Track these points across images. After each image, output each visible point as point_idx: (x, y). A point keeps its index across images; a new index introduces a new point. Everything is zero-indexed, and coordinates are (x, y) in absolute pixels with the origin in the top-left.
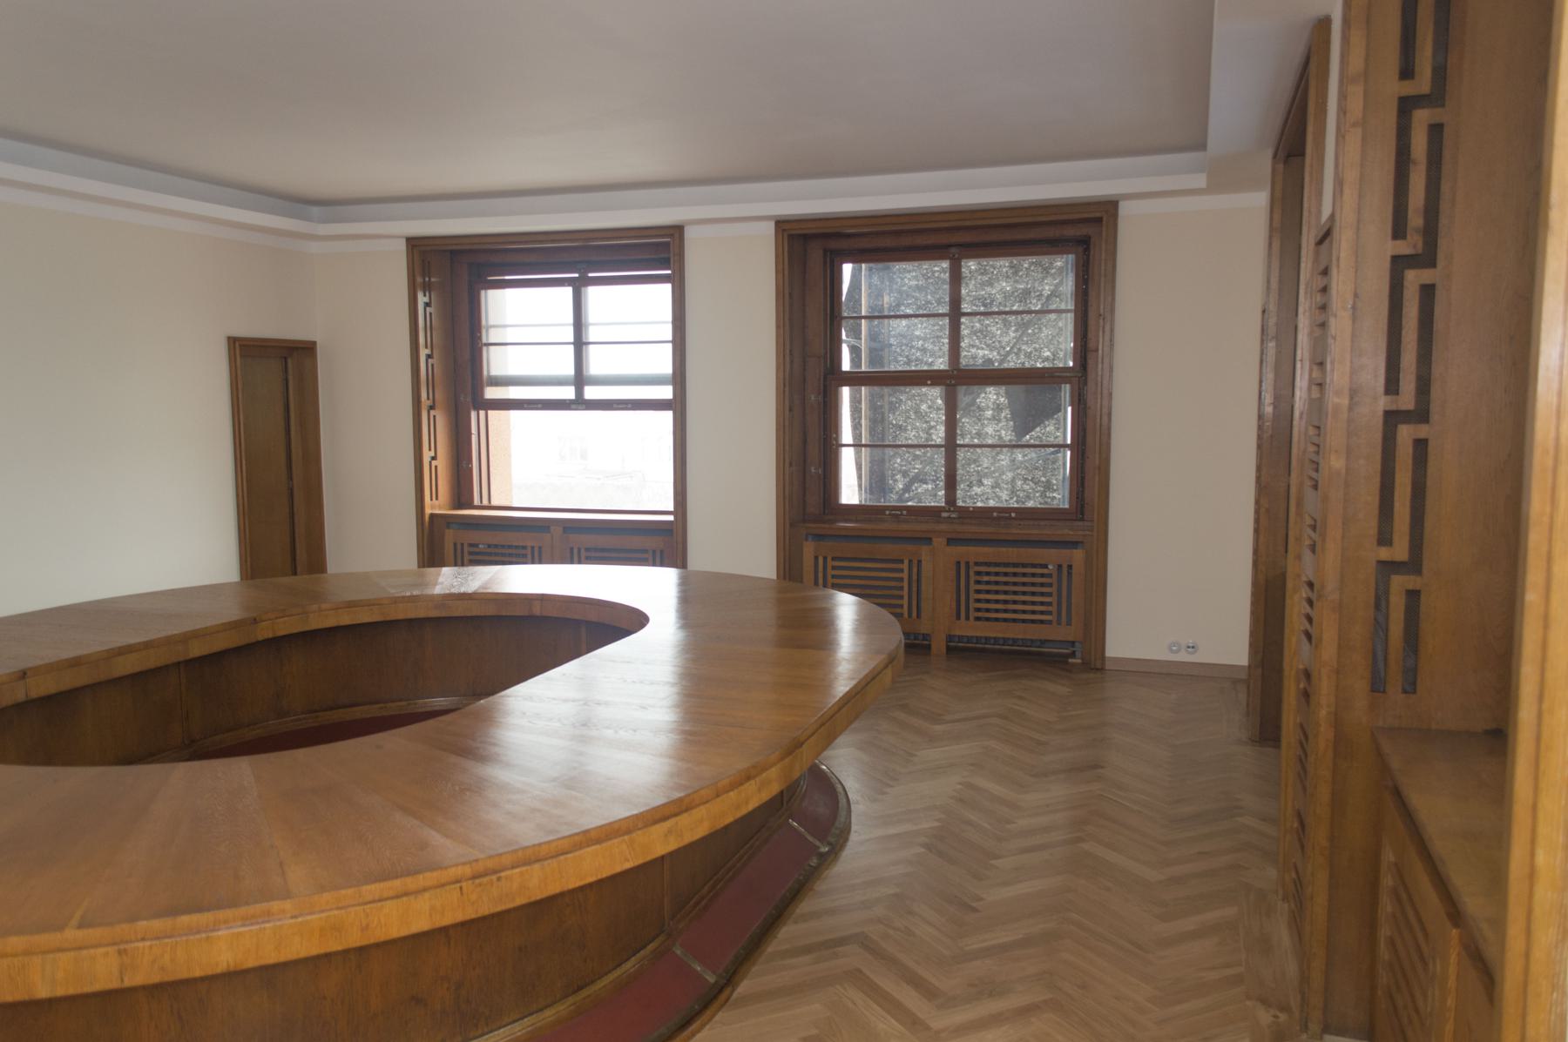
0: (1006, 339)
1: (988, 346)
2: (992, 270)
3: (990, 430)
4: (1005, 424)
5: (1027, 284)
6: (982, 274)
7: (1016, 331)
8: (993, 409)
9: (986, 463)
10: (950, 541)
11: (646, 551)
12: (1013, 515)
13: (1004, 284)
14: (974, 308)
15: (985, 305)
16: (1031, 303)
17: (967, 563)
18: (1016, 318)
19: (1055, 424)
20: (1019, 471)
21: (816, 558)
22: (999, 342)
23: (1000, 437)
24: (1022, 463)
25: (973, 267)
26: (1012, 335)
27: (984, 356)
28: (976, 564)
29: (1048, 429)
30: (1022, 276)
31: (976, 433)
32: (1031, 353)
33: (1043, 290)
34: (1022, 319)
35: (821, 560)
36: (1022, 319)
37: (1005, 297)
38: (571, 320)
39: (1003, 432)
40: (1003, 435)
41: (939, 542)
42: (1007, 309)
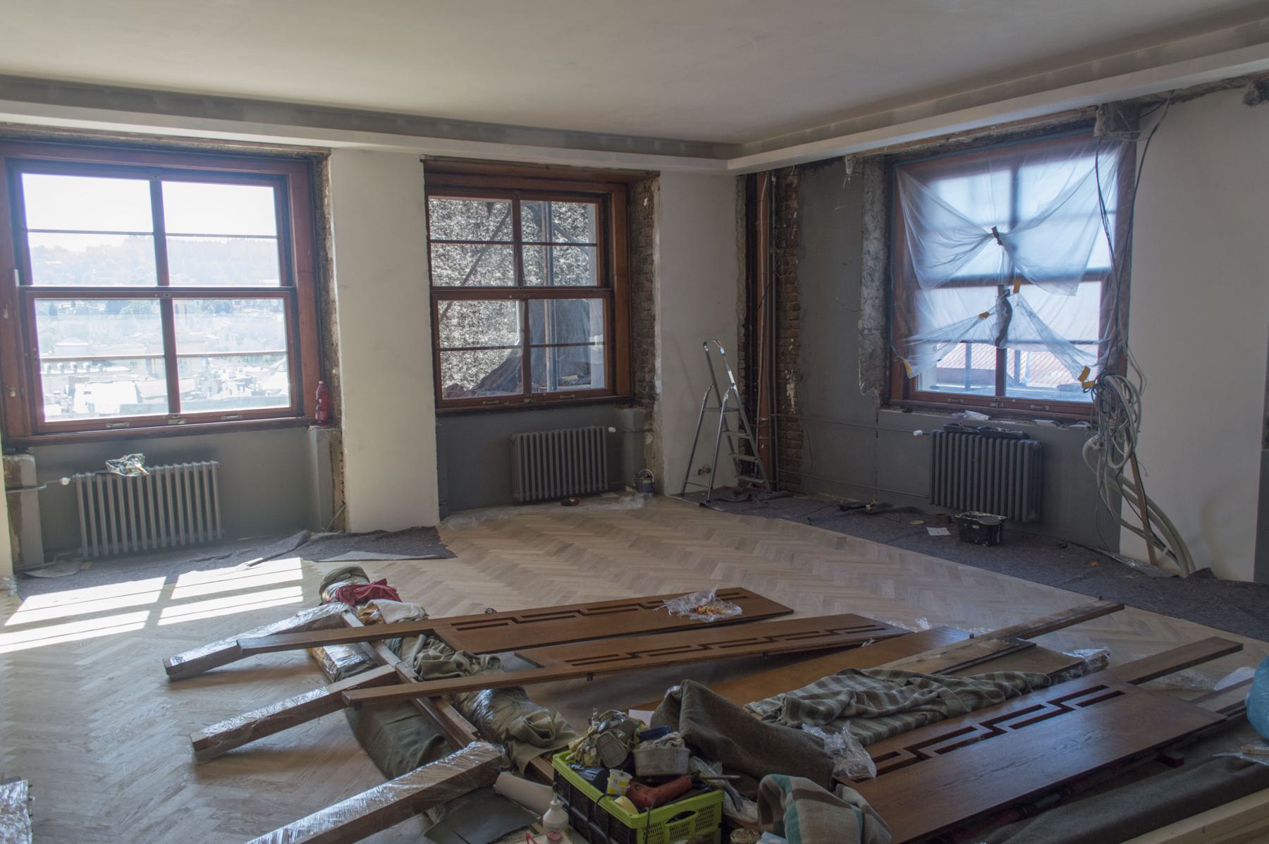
0: (465, 262)
1: (451, 267)
2: (450, 206)
3: (456, 334)
4: (468, 329)
5: (477, 218)
6: (442, 208)
7: (472, 256)
8: (458, 317)
9: (455, 361)
12: (573, 396)
13: (460, 218)
14: (437, 236)
15: (446, 235)
16: (481, 235)
18: (471, 246)
19: (507, 328)
20: (481, 366)
22: (460, 264)
23: (465, 340)
24: (482, 360)
25: (435, 202)
26: (469, 259)
27: (447, 276)
29: (502, 332)
30: (472, 213)
31: (445, 338)
32: (485, 273)
33: (489, 225)
34: (476, 248)
36: (476, 248)
37: (461, 229)
39: (467, 336)
40: (467, 338)
42: (464, 239)
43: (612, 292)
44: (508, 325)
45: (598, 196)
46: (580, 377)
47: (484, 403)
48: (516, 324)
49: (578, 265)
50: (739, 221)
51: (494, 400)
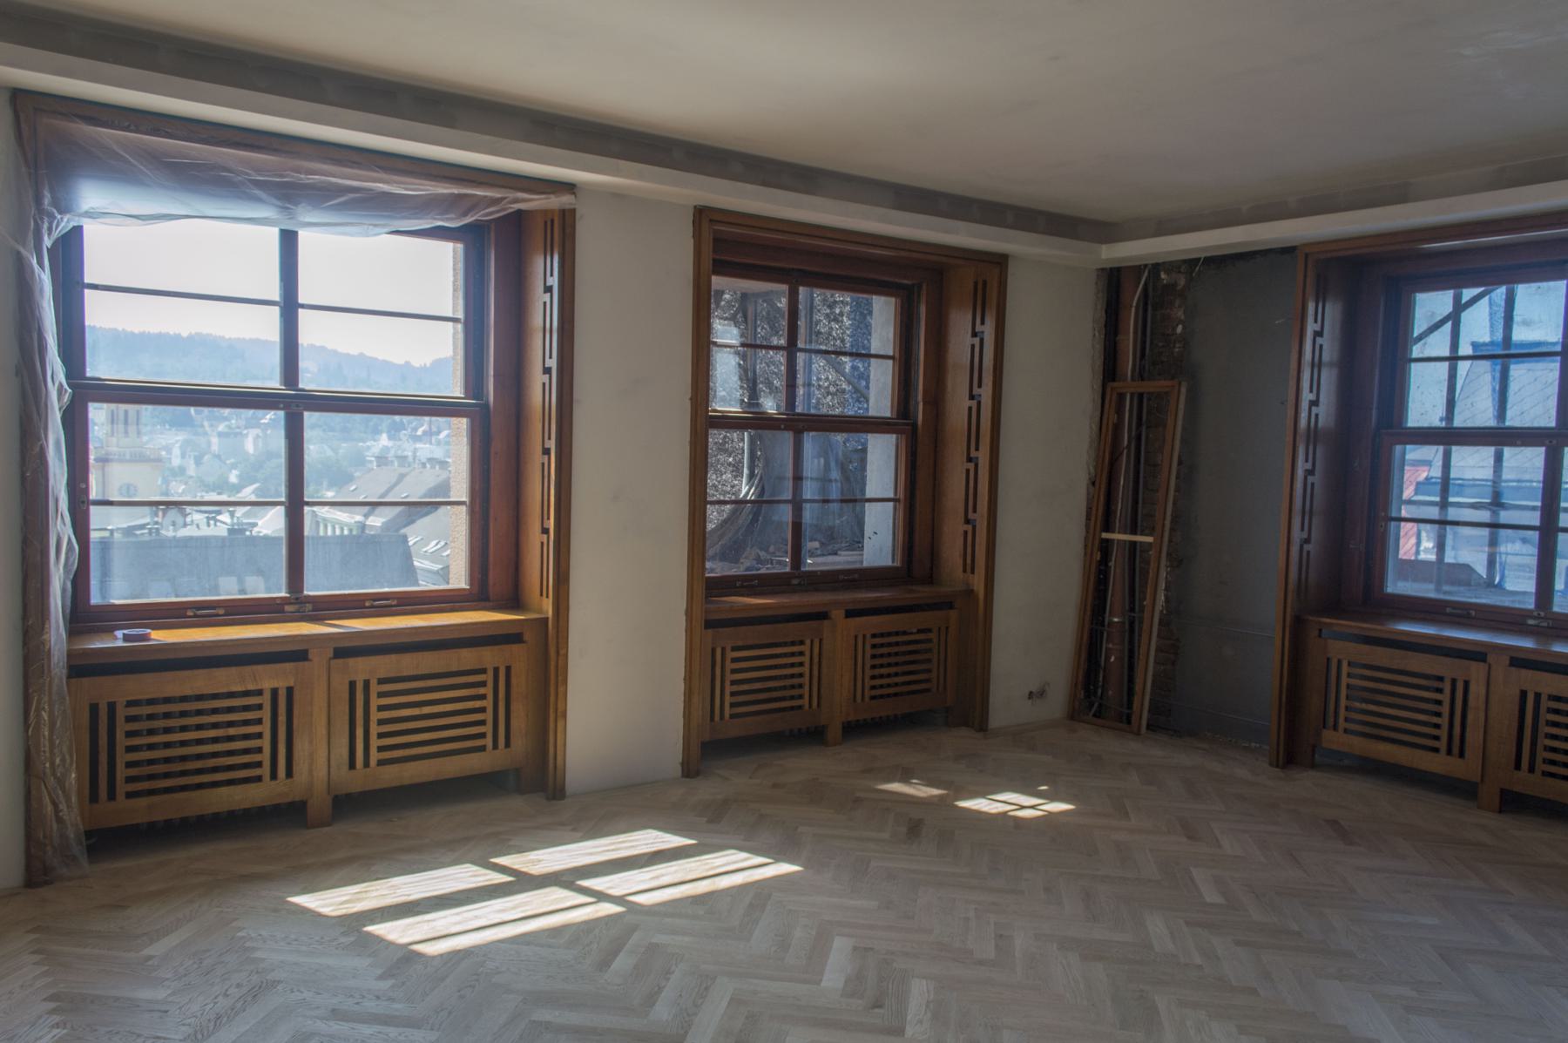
10: (850, 614)
11: (484, 671)
12: (856, 576)
17: (864, 636)
21: (713, 651)
28: (874, 636)
35: (719, 652)
38: (272, 289)
41: (837, 614)
43: (914, 426)
44: (734, 466)
45: (899, 287)
46: (822, 544)
47: (738, 584)
48: (743, 466)
49: (819, 385)
50: (1097, 334)
51: (752, 580)
